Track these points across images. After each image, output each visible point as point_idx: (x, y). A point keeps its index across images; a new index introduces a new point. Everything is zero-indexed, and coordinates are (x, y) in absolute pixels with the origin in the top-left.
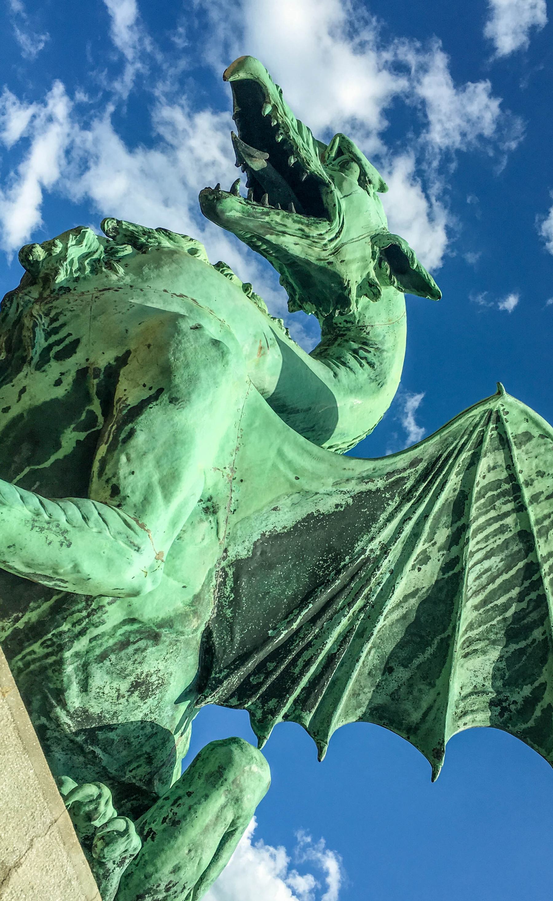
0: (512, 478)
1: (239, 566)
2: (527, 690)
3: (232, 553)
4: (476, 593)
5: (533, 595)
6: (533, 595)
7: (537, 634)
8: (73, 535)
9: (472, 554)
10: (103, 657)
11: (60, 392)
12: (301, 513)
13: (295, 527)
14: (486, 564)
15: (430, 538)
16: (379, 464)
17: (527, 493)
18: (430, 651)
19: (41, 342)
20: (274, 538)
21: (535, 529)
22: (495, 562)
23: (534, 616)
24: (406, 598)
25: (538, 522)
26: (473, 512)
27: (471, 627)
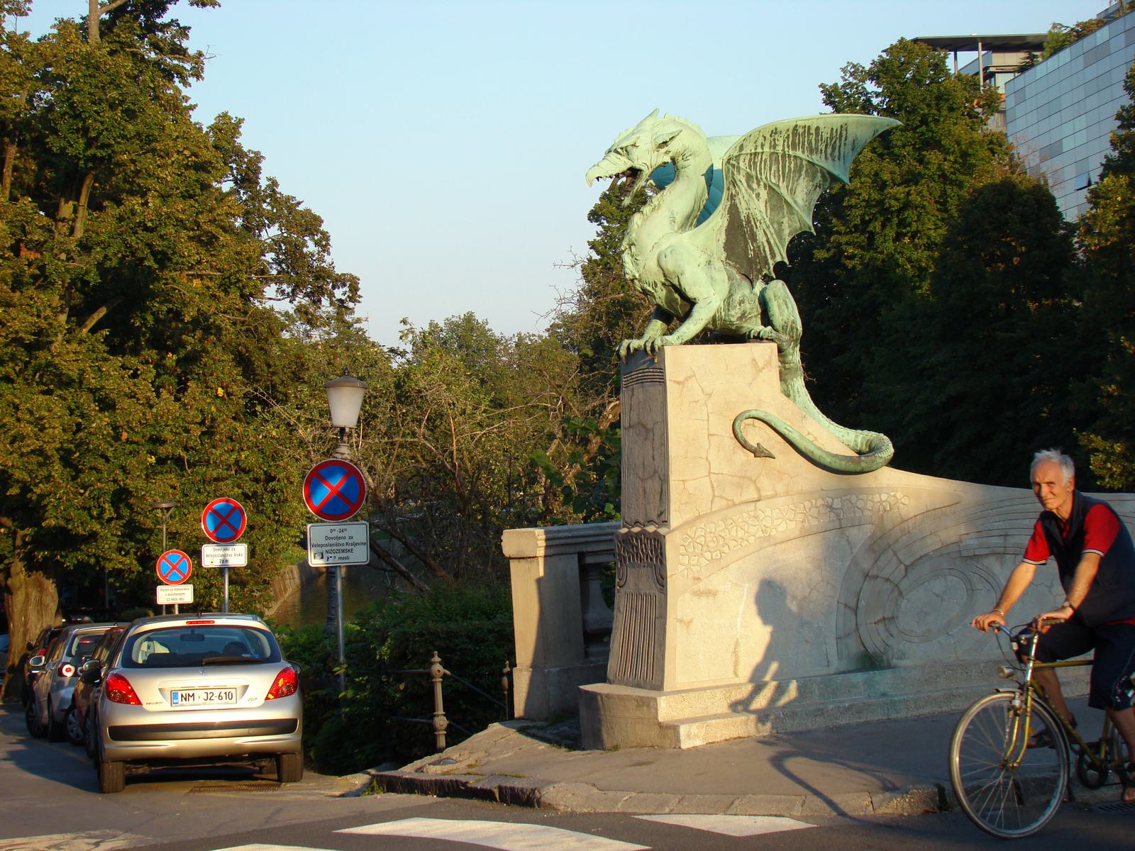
0: (751, 154)
1: (727, 258)
2: (819, 175)
3: (723, 259)
4: (779, 180)
5: (792, 158)
6: (792, 158)
7: (804, 163)
8: (701, 317)
9: (766, 178)
10: (729, 310)
11: (664, 291)
12: (723, 233)
13: (726, 236)
14: (773, 172)
15: (753, 190)
16: (723, 202)
17: (759, 150)
18: (785, 207)
19: (650, 289)
20: (725, 244)
21: (772, 151)
22: (774, 168)
23: (798, 161)
24: (766, 206)
25: (770, 148)
26: (753, 173)
27: (787, 187)
